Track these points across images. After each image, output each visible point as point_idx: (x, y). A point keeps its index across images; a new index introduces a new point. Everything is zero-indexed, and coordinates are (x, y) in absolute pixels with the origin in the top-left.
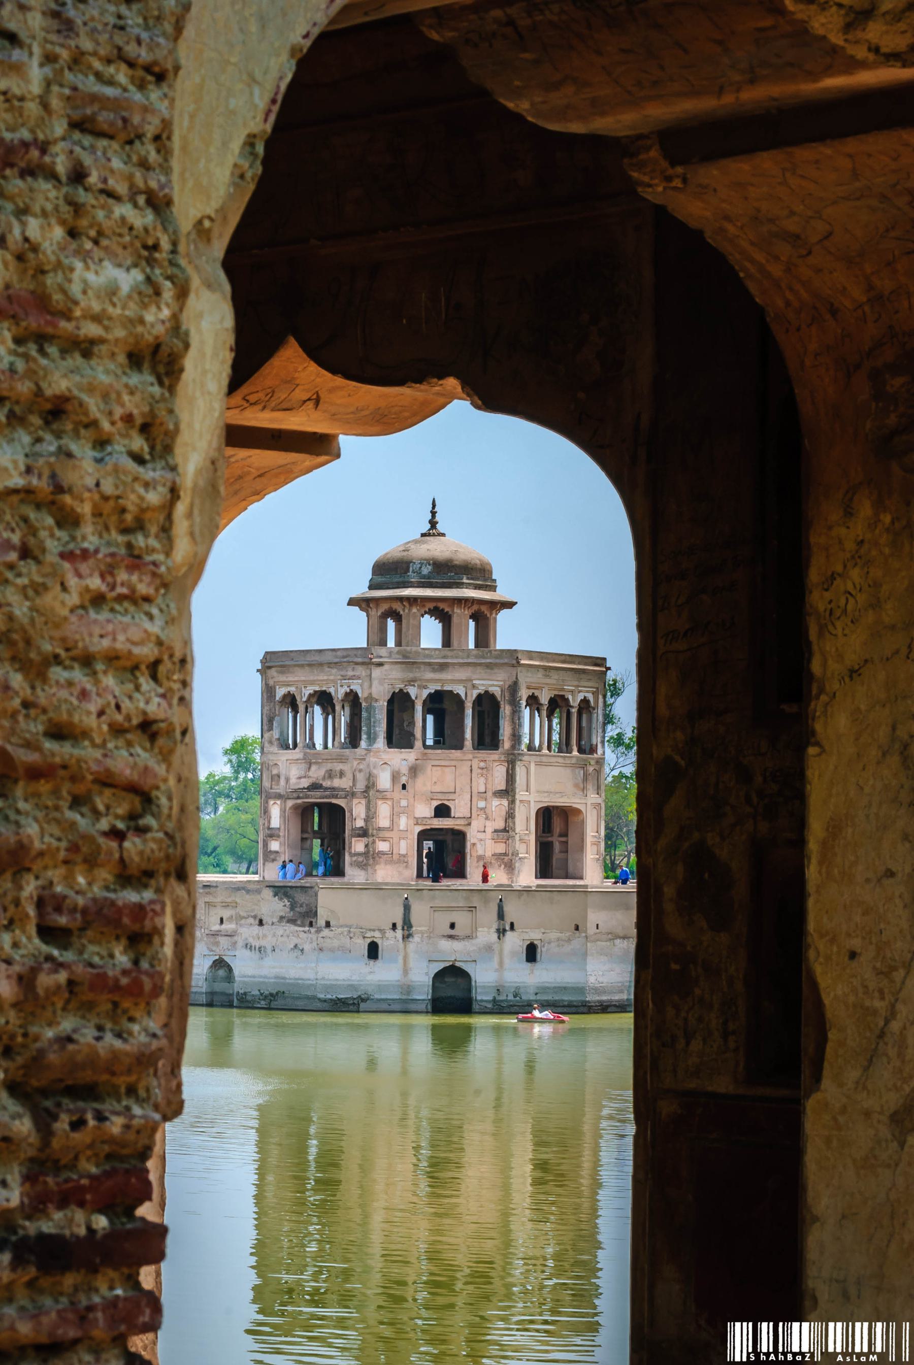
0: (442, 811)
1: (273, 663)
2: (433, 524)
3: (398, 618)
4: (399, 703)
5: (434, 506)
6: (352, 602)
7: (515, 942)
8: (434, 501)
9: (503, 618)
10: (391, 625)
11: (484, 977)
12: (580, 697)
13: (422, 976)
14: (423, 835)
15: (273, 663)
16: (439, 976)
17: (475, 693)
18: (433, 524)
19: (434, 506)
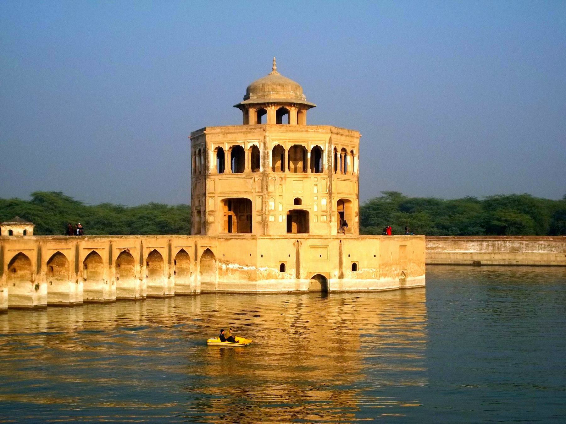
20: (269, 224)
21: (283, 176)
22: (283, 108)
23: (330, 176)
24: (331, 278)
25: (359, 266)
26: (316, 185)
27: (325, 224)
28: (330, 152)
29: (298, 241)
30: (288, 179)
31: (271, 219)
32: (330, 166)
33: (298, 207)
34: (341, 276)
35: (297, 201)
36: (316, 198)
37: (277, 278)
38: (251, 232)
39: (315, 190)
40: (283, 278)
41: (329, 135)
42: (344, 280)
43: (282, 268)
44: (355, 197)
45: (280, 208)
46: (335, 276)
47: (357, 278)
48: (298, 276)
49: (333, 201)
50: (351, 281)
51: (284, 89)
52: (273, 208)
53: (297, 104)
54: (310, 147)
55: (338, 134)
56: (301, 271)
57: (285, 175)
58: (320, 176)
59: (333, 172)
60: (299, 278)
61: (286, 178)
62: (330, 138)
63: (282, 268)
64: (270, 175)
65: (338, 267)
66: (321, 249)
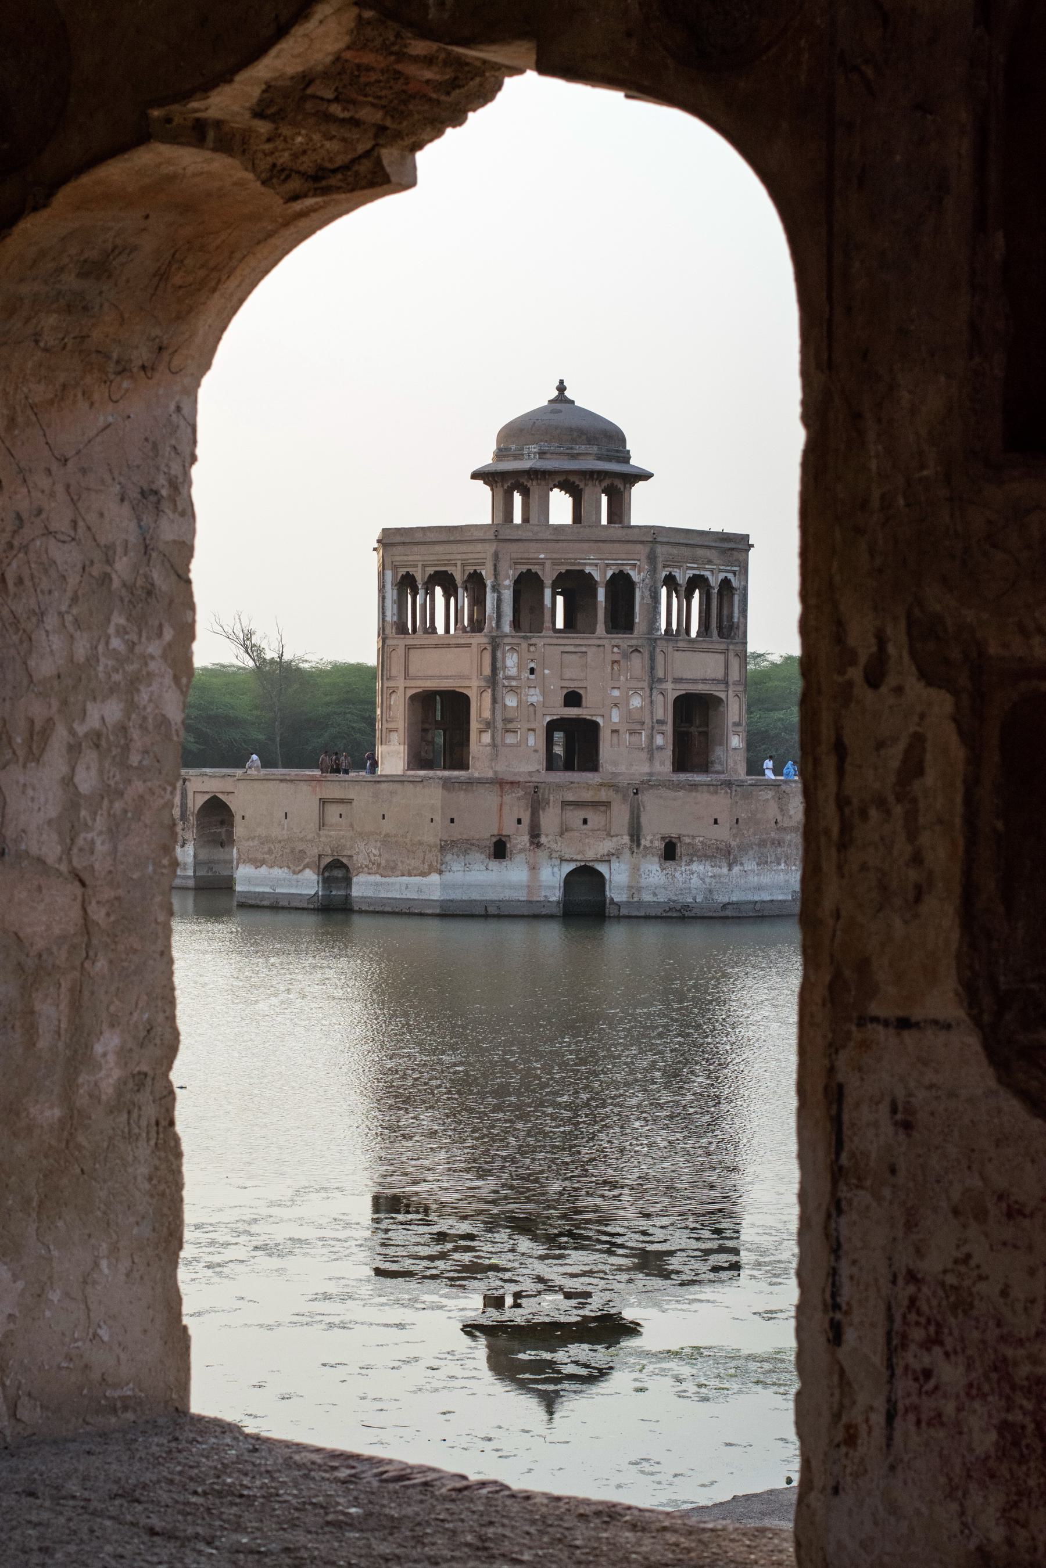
0: (573, 699)
1: (392, 541)
3: (526, 493)
4: (527, 586)
6: (475, 476)
7: (652, 839)
9: (638, 491)
10: (517, 498)
11: (618, 879)
12: (722, 576)
13: (551, 880)
14: (552, 727)
15: (392, 541)
16: (570, 879)
17: (609, 573)
18: (561, 388)
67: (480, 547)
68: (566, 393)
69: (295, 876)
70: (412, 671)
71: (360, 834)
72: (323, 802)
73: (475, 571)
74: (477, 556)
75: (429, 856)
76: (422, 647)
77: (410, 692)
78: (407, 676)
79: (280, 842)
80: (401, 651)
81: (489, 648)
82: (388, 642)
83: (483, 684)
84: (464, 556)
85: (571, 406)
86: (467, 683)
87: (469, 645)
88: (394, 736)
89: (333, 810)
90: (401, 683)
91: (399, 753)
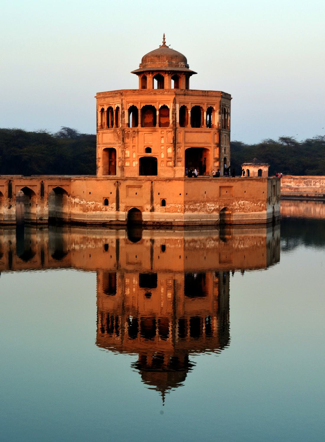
2: (164, 43)
5: (164, 36)
8: (164, 35)
18: (164, 43)
19: (164, 36)
20: (125, 168)
21: (136, 130)
22: (159, 74)
23: (175, 130)
24: (144, 211)
25: (167, 201)
26: (163, 137)
27: (170, 168)
28: (174, 110)
29: (118, 182)
30: (140, 133)
31: (127, 164)
32: (174, 122)
33: (149, 155)
34: (152, 210)
35: (148, 150)
36: (162, 147)
37: (101, 210)
38: (116, 174)
39: (163, 142)
40: (106, 210)
41: (174, 96)
42: (155, 213)
43: (106, 203)
44: (213, 145)
45: (134, 156)
46: (147, 209)
47: (166, 212)
48: (118, 209)
49: (178, 150)
50: (160, 214)
51: (159, 59)
52: (128, 156)
53: (168, 71)
54: (158, 106)
55: (185, 95)
56: (120, 205)
57: (138, 129)
58: (169, 129)
59: (178, 125)
60: (119, 211)
61: (138, 132)
62: (175, 99)
63: (106, 203)
64: (126, 130)
65: (150, 202)
66: (137, 188)
67: (214, 99)
68: (166, 44)
69: (210, 214)
70: (187, 140)
71: (236, 198)
72: (220, 187)
73: (211, 107)
74: (213, 101)
75: (262, 205)
76: (191, 132)
77: (187, 148)
78: (185, 143)
79: (203, 202)
80: (183, 133)
81: (218, 134)
82: (177, 130)
83: (216, 146)
84: (208, 101)
85: (167, 48)
86: (210, 145)
87: (209, 132)
88: (179, 164)
89: (224, 192)
90: (183, 145)
91: (182, 170)
